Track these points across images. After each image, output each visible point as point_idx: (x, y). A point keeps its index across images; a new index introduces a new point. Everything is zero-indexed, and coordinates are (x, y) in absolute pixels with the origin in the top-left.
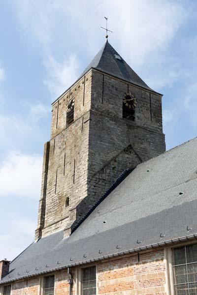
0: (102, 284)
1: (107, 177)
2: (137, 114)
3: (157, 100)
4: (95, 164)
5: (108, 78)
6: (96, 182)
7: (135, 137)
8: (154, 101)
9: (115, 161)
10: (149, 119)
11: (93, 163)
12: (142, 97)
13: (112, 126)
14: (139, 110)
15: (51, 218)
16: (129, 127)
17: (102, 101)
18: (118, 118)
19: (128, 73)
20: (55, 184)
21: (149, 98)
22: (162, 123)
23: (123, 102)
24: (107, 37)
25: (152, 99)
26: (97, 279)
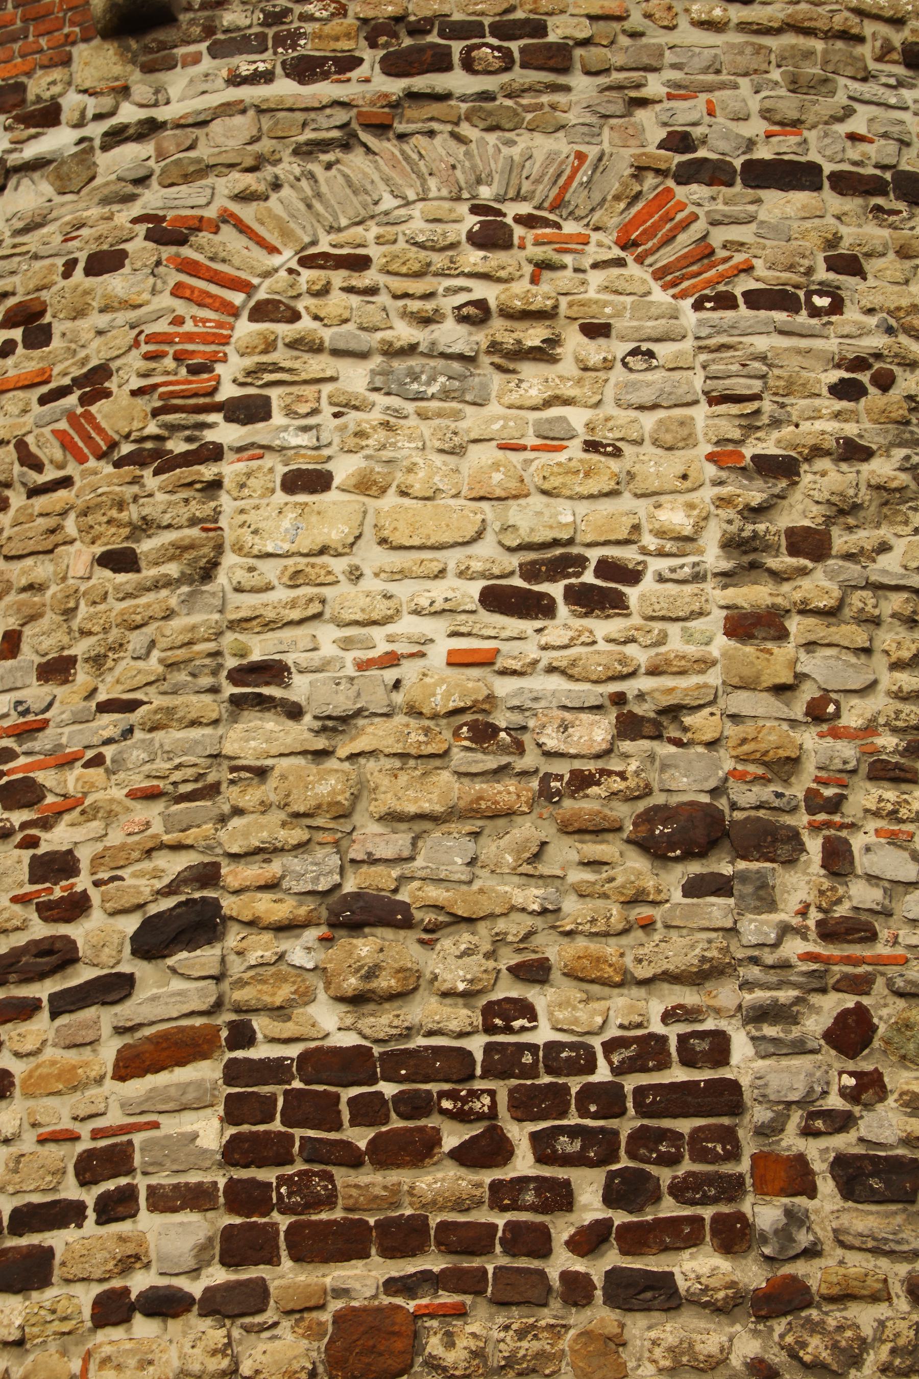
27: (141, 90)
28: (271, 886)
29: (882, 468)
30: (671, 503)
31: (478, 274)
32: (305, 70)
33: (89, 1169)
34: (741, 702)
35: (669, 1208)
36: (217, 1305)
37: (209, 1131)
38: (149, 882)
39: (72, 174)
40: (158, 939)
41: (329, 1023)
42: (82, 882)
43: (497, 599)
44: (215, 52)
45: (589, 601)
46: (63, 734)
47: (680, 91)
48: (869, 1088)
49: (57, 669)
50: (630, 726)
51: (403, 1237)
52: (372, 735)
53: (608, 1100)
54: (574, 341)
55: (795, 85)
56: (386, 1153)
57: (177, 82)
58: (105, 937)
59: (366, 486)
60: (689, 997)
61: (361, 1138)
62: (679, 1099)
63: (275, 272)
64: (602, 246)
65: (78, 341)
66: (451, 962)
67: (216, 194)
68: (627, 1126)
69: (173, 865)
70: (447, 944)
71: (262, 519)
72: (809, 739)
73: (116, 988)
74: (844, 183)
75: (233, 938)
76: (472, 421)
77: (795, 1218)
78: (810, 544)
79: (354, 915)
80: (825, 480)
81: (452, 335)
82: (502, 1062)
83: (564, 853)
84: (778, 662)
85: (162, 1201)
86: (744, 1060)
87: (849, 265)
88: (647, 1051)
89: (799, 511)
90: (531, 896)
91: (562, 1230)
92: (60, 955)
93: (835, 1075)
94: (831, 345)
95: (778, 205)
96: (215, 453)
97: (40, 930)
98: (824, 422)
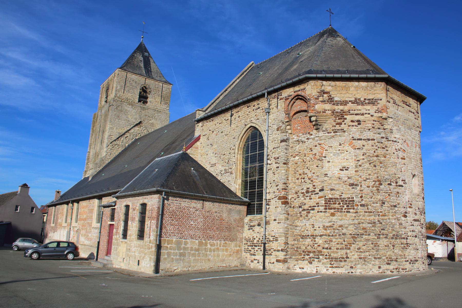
2: (149, 100)
5: (130, 75)
7: (146, 115)
13: (129, 109)
18: (134, 102)
19: (150, 68)
21: (161, 88)
29: (365, 160)
30: (351, 164)
32: (328, 133)
33: (317, 204)
36: (324, 212)
37: (324, 202)
38: (320, 187)
39: (313, 139)
40: (320, 191)
41: (331, 196)
43: (341, 170)
45: (346, 170)
46: (314, 177)
47: (353, 133)
48: (362, 200)
49: (314, 173)
50: (349, 178)
51: (335, 209)
52: (333, 178)
53: (347, 201)
56: (334, 204)
57: (320, 133)
58: (317, 190)
59: (332, 162)
62: (351, 201)
63: (326, 148)
64: (348, 145)
66: (338, 193)
67: (322, 142)
68: (348, 202)
69: (321, 186)
71: (326, 165)
72: (360, 179)
73: (318, 193)
74: (364, 140)
78: (360, 166)
79: (332, 190)
81: (338, 152)
82: (340, 199)
83: (344, 186)
84: (358, 173)
85: (321, 206)
86: (355, 199)
87: (364, 146)
88: (349, 198)
89: (360, 163)
90: (342, 189)
91: (344, 208)
92: (315, 191)
93: (360, 199)
94: (362, 152)
95: (359, 141)
98: (362, 157)
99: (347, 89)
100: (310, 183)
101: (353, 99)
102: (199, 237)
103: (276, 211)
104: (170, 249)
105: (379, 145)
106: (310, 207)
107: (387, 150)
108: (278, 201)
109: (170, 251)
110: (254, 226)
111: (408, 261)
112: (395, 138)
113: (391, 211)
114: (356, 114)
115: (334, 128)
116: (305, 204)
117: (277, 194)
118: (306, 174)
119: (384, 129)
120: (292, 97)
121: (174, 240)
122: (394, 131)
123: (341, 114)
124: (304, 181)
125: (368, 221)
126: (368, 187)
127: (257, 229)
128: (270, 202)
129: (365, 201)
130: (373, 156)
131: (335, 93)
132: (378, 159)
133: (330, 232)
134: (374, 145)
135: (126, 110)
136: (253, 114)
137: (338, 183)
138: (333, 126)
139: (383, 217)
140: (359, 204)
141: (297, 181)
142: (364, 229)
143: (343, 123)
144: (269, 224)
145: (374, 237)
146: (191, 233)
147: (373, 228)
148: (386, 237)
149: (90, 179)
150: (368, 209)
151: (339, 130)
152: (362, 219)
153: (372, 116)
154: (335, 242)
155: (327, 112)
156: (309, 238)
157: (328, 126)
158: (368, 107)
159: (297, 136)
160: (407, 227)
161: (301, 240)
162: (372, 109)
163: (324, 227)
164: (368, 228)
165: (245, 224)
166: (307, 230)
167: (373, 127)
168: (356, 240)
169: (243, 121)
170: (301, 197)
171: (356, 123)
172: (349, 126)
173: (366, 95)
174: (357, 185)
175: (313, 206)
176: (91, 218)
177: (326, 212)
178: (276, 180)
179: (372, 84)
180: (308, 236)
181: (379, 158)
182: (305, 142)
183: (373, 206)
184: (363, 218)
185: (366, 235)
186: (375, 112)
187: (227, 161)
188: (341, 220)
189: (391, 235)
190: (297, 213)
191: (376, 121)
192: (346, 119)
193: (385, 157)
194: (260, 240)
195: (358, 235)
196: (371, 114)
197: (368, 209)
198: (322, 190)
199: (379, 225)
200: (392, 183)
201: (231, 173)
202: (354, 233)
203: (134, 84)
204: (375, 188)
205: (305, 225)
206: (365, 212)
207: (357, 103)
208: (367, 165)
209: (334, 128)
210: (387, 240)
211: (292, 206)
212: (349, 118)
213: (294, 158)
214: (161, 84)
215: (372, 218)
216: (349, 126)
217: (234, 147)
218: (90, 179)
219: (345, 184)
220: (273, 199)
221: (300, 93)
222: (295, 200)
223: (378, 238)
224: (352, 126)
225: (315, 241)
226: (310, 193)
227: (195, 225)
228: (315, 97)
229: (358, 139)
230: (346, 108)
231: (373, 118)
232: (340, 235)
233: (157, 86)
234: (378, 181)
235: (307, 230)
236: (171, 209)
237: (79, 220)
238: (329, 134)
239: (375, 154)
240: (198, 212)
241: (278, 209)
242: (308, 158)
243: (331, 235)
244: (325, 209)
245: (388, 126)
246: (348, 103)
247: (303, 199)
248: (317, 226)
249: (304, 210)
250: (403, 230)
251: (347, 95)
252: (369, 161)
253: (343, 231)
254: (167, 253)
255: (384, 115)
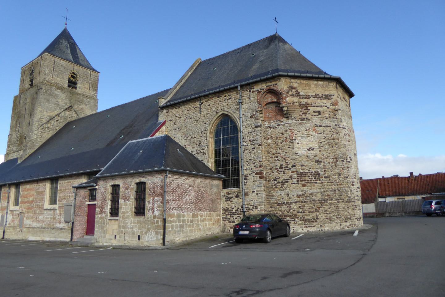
0: (22, 193)
1: (52, 126)
3: (96, 76)
4: (43, 118)
5: (58, 60)
6: (43, 129)
8: (93, 76)
9: (59, 116)
10: (87, 88)
11: (42, 118)
12: (84, 74)
13: (59, 93)
14: (81, 83)
15: (15, 148)
16: (73, 94)
17: (53, 76)
18: (64, 87)
20: (19, 126)
21: (89, 75)
22: (97, 91)
23: (69, 77)
24: (66, 24)
25: (91, 76)
26: (20, 191)
27: (287, 121)
28: (298, 164)
29: (326, 142)
30: (316, 145)
31: (307, 133)
32: (296, 121)
33: (290, 177)
34: (320, 155)
35: (317, 179)
36: (297, 183)
37: (296, 176)
38: (292, 164)
40: (292, 167)
41: (301, 171)
42: (288, 164)
43: (308, 150)
44: (292, 119)
45: (312, 150)
46: (287, 156)
47: (315, 121)
48: (326, 173)
50: (315, 156)
51: (305, 180)
52: (302, 157)
53: (314, 174)
54: (311, 136)
55: (321, 121)
56: (304, 177)
57: (289, 121)
58: (290, 166)
60: (317, 169)
61: (303, 176)
63: (296, 132)
64: (312, 130)
65: (285, 136)
66: (307, 168)
67: (292, 128)
68: (315, 175)
69: (293, 163)
70: (306, 167)
72: (323, 157)
73: (290, 169)
74: (324, 126)
75: (296, 167)
76: (306, 140)
77: (322, 179)
78: (322, 147)
79: (302, 166)
80: (323, 143)
81: (305, 136)
82: (309, 173)
83: (311, 163)
84: (321, 152)
85: (294, 179)
87: (324, 131)
88: (316, 172)
89: (322, 145)
90: (310, 165)
91: (312, 180)
92: (287, 167)
94: (323, 136)
95: (321, 128)
96: (293, 142)
97: (286, 166)
98: (323, 140)
99: (309, 86)
100: (283, 161)
101: (314, 94)
102: (193, 210)
103: (254, 184)
104: (173, 222)
105: (334, 130)
106: (284, 180)
107: (339, 135)
108: (255, 176)
109: (173, 224)
110: (232, 198)
111: (356, 219)
112: (344, 125)
113: (344, 181)
114: (317, 106)
115: (300, 117)
116: (279, 178)
117: (254, 170)
118: (279, 153)
119: (337, 118)
120: (265, 90)
121: (176, 213)
122: (343, 120)
123: (306, 106)
124: (278, 159)
125: (330, 189)
126: (329, 163)
127: (235, 200)
128: (248, 177)
129: (328, 174)
130: (331, 139)
131: (301, 89)
132: (334, 142)
133: (303, 200)
134: (331, 131)
135: (56, 94)
136: (225, 104)
137: (307, 161)
138: (300, 116)
139: (340, 186)
140: (323, 176)
141: (271, 159)
142: (328, 195)
143: (308, 113)
144: (248, 195)
145: (335, 201)
146: (187, 206)
147: (334, 195)
148: (343, 202)
149: (19, 162)
150: (330, 180)
151: (305, 118)
152: (326, 188)
153: (328, 108)
154: (307, 207)
155: (295, 104)
156: (285, 205)
157: (296, 115)
158: (325, 101)
159: (269, 123)
160: (355, 193)
161: (277, 207)
162: (327, 103)
163: (297, 195)
164: (331, 195)
165: (222, 197)
166: (283, 199)
167: (330, 117)
168: (323, 204)
169: (214, 109)
170: (275, 172)
171: (317, 114)
172: (312, 115)
173: (322, 91)
174: (321, 162)
175: (287, 179)
176: (43, 200)
177: (298, 183)
178: (253, 159)
179: (326, 83)
180: (284, 203)
181: (335, 141)
182: (276, 128)
183: (333, 178)
184: (327, 187)
185: (330, 200)
186: (330, 105)
187: (198, 143)
188: (311, 189)
189: (346, 199)
190: (273, 185)
191: (331, 112)
192: (309, 110)
193: (338, 140)
194: (239, 210)
195: (324, 200)
196: (328, 106)
197: (330, 180)
198: (294, 166)
199: (338, 192)
200: (344, 160)
201: (204, 154)
202: (321, 199)
203: (62, 69)
204: (334, 164)
205: (281, 194)
206: (328, 182)
207: (317, 97)
208: (327, 147)
209: (300, 117)
210: (344, 203)
211: (268, 179)
212: (312, 109)
213: (267, 141)
214: (89, 72)
215: (333, 187)
216: (312, 115)
217: (205, 132)
218: (19, 162)
219: (312, 161)
220: (250, 174)
221: (272, 87)
222: (270, 174)
223: (338, 202)
224: (315, 115)
225: (290, 207)
226: (284, 169)
227: (190, 199)
228: (286, 91)
229: (320, 126)
230: (309, 101)
231: (329, 110)
232: (310, 201)
233: (85, 73)
234: (336, 158)
235: (283, 199)
236: (172, 186)
237: (21, 203)
238: (297, 122)
239: (332, 138)
240: (191, 188)
241: (256, 183)
242: (280, 141)
243: (304, 201)
244: (298, 181)
245: (339, 116)
246: (310, 97)
247: (277, 173)
248: (292, 195)
249: (279, 183)
250: (352, 195)
251: (309, 91)
252: (328, 143)
253: (313, 198)
254: (172, 225)
255: (337, 107)
